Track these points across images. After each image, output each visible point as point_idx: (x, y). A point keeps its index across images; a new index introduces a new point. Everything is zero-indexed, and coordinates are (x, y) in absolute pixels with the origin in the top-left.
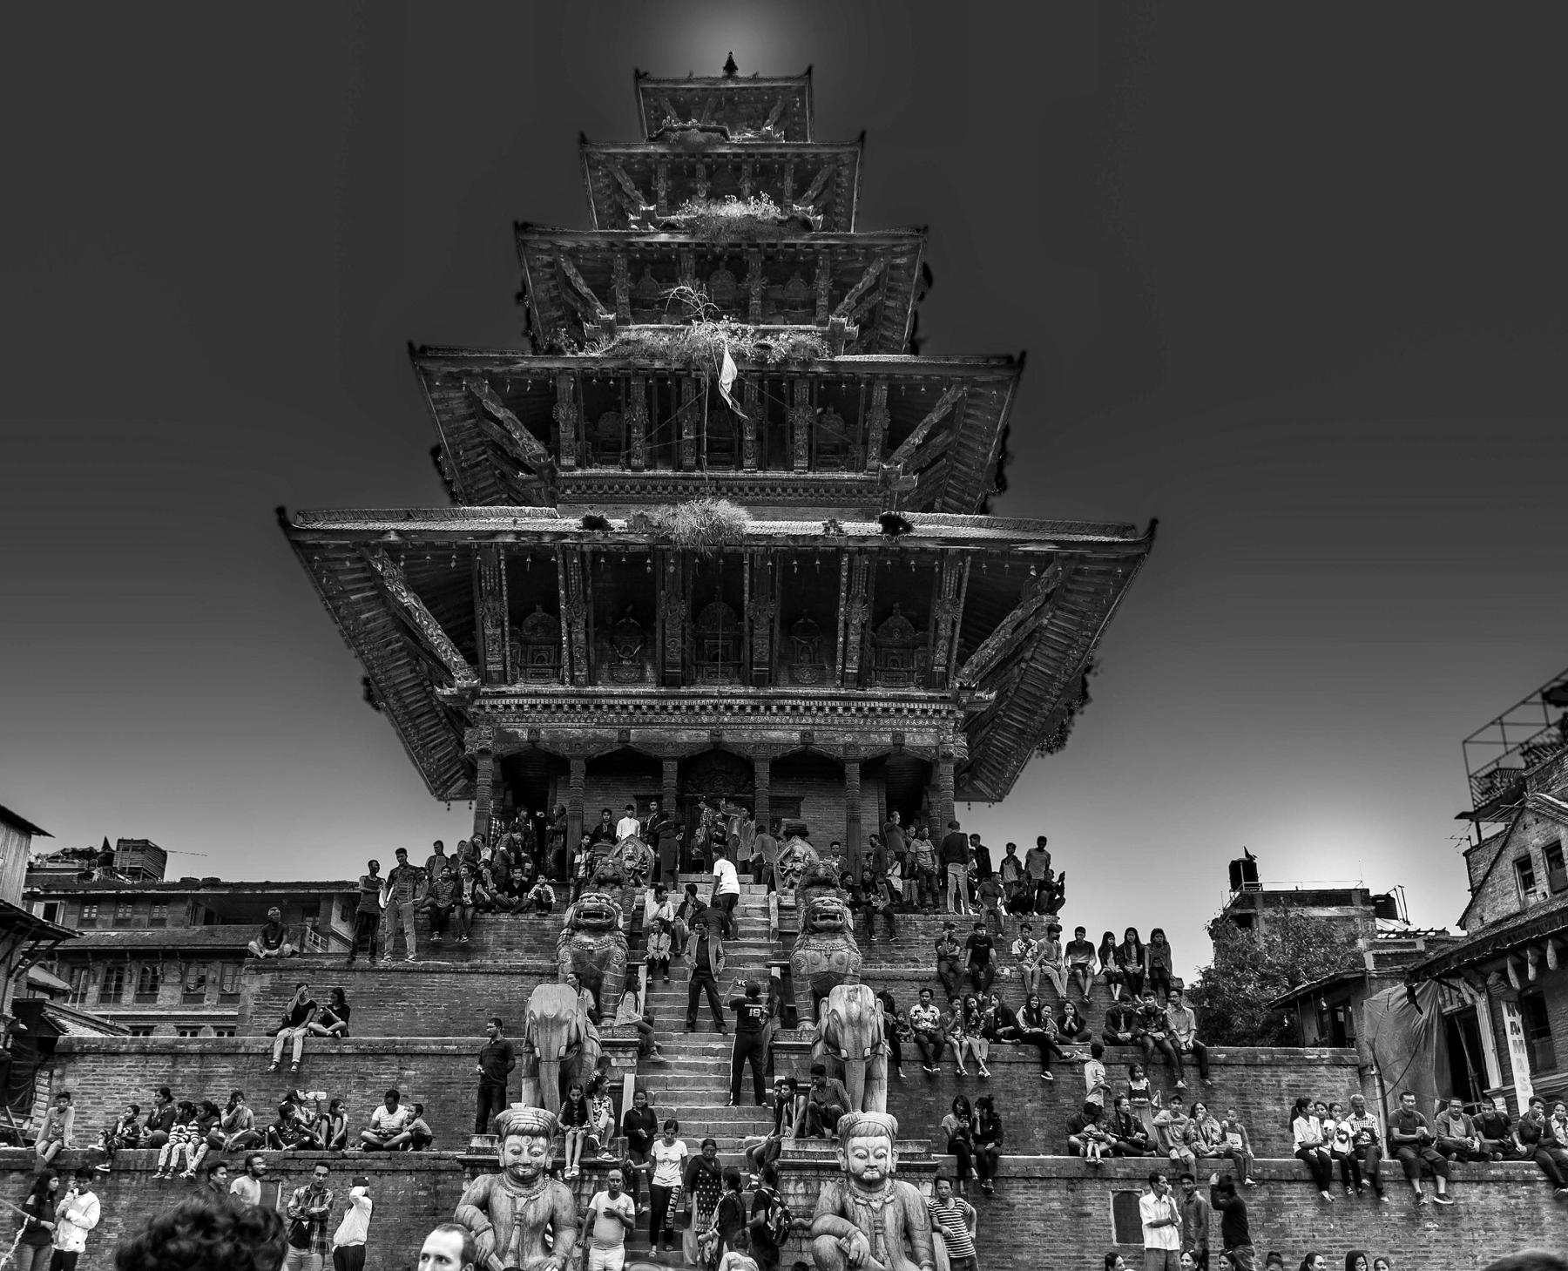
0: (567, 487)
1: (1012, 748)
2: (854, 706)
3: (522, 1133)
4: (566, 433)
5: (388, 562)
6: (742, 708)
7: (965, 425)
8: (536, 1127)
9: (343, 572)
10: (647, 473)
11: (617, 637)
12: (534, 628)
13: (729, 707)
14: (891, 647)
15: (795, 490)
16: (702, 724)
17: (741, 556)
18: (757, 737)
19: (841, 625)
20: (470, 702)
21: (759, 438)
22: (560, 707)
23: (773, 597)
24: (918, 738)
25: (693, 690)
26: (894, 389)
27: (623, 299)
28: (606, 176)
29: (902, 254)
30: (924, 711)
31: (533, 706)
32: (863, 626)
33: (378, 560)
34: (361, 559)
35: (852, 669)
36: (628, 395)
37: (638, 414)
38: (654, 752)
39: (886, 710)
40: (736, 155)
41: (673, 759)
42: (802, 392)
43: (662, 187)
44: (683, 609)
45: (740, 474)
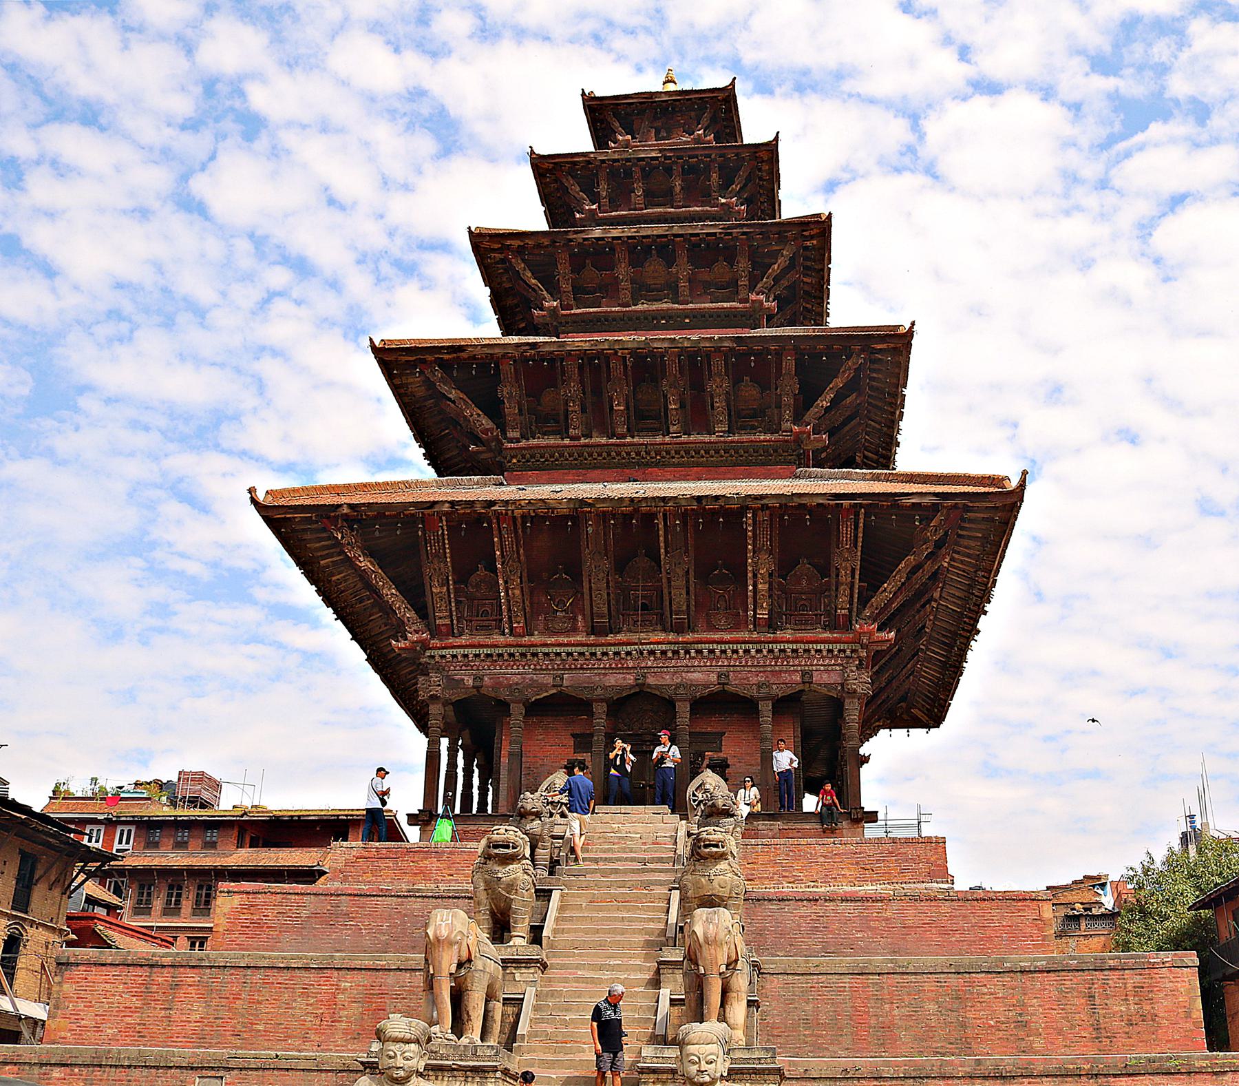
0: (513, 457)
1: (938, 678)
3: (396, 1040)
4: (511, 410)
5: (346, 530)
6: (664, 653)
7: (871, 388)
8: (408, 1036)
9: (310, 541)
10: (583, 441)
12: (478, 586)
13: (652, 652)
15: (717, 452)
16: (628, 668)
17: (653, 516)
19: (750, 575)
21: (682, 406)
23: (687, 551)
24: (825, 676)
25: (619, 637)
27: (566, 287)
28: (556, 181)
29: (812, 237)
30: (830, 651)
32: (771, 575)
33: (338, 530)
34: (324, 530)
35: (763, 614)
37: (574, 388)
38: (585, 695)
39: (793, 651)
41: (602, 701)
42: (718, 364)
43: (603, 189)
44: (606, 564)
45: (667, 439)
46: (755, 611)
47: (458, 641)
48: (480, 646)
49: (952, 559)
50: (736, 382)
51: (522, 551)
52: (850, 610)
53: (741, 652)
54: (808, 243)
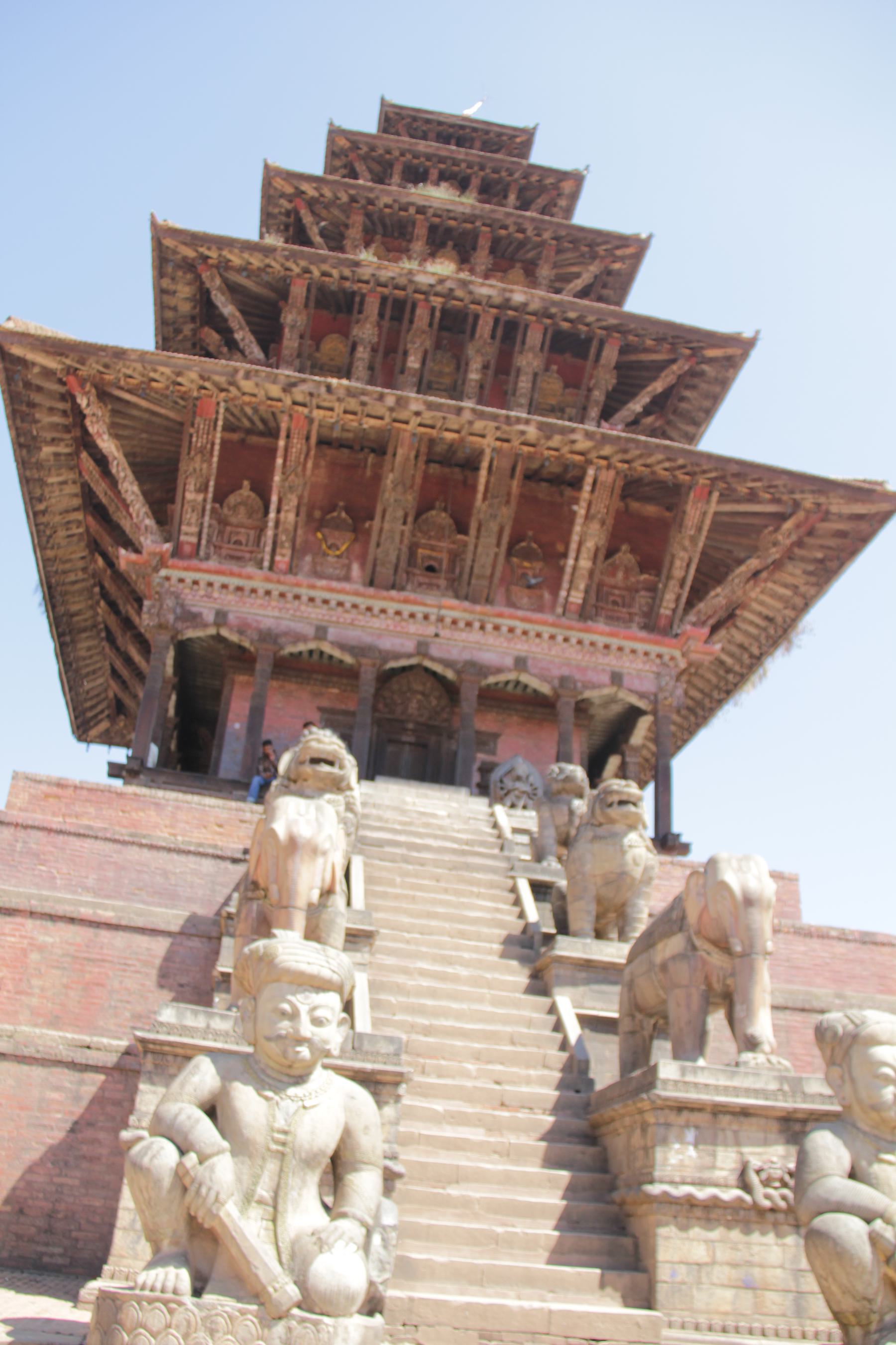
2: (574, 636)
4: (290, 342)
5: (93, 398)
6: (454, 622)
11: (326, 531)
12: (234, 508)
14: (614, 587)
18: (466, 656)
20: (156, 570)
22: (254, 591)
23: (508, 502)
25: (403, 594)
26: (624, 350)
28: (345, 166)
29: (622, 259)
30: (646, 654)
31: (224, 586)
35: (577, 597)
37: (366, 331)
39: (607, 647)
40: (470, 166)
42: (534, 337)
44: (410, 499)
46: (569, 591)
47: (204, 565)
48: (232, 574)
49: (762, 592)
50: (547, 369)
51: (310, 464)
52: (674, 611)
53: (546, 636)
54: (617, 266)
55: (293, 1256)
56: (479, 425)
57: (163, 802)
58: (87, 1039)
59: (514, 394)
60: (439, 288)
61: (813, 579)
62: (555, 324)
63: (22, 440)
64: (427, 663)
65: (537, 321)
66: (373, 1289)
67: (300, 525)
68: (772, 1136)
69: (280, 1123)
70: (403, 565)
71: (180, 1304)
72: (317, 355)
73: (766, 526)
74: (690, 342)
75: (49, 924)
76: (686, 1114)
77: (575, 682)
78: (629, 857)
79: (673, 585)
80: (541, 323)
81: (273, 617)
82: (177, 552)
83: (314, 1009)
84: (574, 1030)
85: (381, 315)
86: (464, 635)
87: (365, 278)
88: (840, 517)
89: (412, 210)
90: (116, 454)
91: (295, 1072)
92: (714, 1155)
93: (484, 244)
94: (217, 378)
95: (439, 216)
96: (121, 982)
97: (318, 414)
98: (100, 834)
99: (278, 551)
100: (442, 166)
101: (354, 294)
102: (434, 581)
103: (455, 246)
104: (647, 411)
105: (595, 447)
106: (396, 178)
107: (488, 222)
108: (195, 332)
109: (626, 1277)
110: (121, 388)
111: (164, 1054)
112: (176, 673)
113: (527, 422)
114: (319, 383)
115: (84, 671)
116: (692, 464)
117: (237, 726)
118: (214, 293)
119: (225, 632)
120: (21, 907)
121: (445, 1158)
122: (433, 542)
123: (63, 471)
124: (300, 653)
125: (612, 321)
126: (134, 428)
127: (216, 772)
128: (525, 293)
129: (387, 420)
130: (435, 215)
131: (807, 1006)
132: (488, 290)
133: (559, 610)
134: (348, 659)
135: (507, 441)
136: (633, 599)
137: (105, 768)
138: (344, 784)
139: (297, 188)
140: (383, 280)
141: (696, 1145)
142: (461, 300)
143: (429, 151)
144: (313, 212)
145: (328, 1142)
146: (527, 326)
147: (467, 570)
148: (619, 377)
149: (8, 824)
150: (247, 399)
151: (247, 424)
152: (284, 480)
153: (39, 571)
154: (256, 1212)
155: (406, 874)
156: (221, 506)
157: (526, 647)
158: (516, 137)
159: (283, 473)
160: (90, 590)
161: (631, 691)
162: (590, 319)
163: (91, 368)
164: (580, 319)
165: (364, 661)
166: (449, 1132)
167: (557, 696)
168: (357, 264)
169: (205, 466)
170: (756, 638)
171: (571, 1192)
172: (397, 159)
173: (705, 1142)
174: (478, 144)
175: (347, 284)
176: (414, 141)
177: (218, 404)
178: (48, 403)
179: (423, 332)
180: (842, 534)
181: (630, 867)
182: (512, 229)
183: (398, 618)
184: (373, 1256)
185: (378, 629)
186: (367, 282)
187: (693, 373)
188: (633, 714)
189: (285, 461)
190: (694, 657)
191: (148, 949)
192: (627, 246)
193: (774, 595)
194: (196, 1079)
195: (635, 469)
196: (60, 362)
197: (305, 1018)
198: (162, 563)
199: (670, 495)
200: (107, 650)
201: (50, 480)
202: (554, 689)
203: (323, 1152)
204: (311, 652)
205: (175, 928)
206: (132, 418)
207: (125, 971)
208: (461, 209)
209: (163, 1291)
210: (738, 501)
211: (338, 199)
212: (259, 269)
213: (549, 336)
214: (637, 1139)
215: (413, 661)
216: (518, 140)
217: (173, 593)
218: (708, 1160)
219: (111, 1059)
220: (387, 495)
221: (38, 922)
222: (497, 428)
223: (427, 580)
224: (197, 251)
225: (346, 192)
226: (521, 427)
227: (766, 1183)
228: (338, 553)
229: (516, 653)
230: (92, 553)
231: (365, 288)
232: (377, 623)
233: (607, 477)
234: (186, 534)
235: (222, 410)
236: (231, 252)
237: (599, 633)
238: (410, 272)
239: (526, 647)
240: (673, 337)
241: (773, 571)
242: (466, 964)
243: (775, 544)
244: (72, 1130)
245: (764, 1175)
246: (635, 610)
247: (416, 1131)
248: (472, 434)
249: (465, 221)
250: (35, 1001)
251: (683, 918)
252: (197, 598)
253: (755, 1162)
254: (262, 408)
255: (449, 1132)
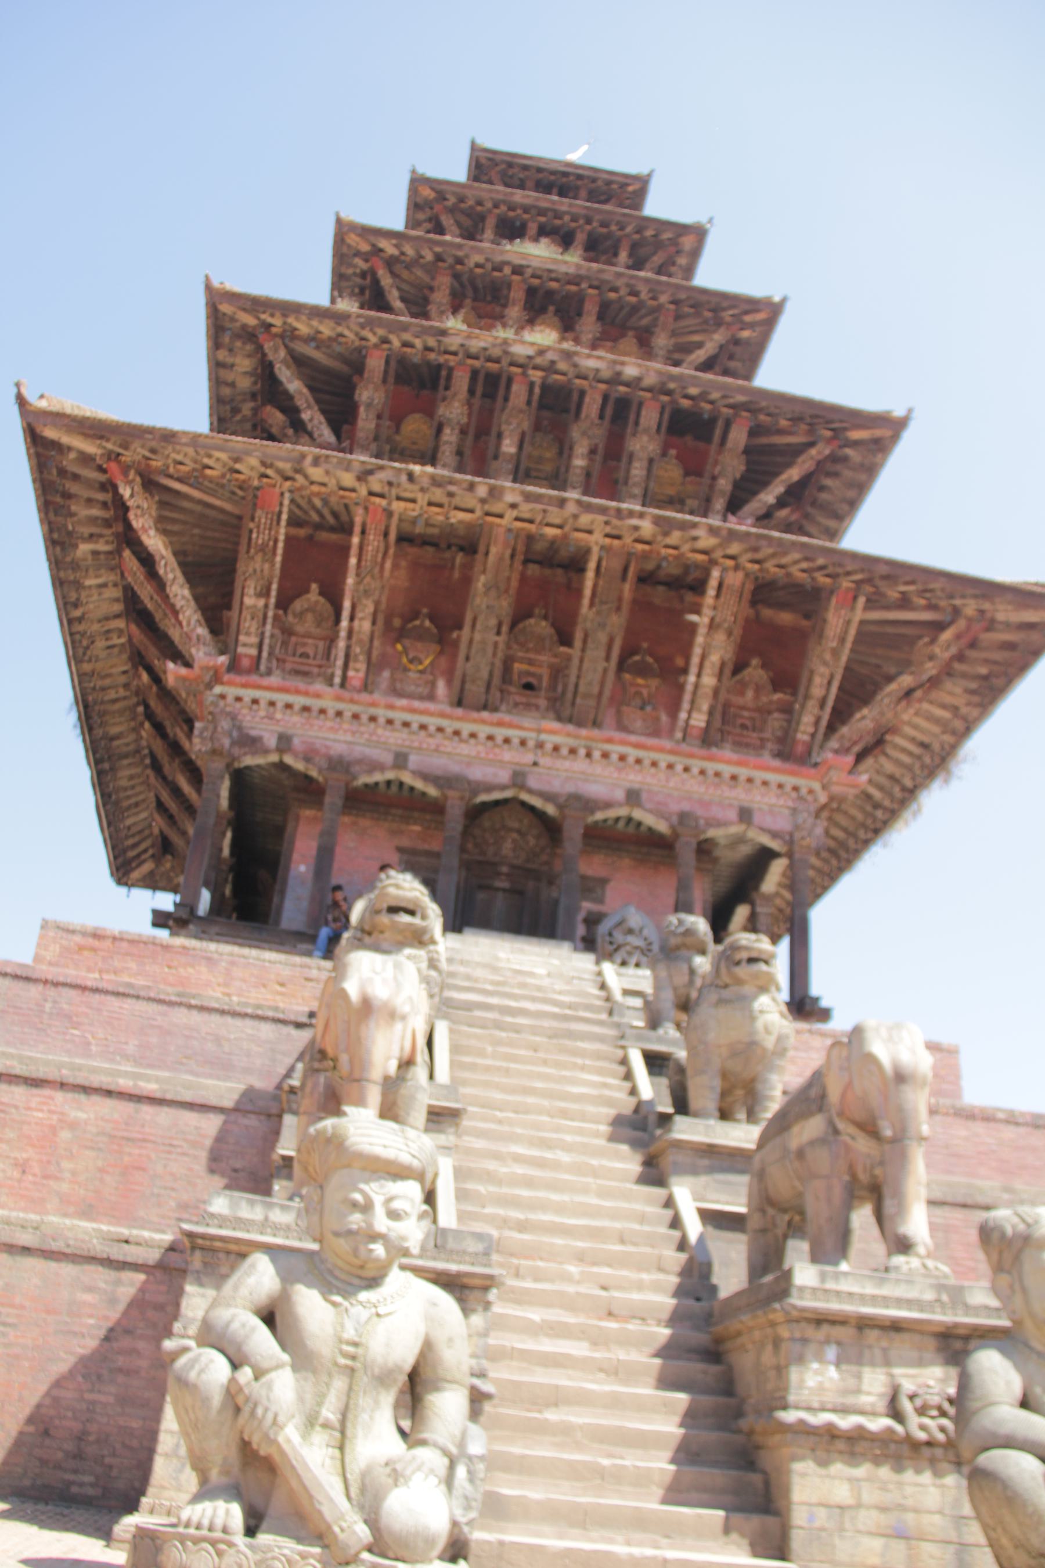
2: (696, 765)
4: (366, 422)
5: (138, 488)
6: (556, 749)
11: (407, 642)
12: (301, 615)
14: (743, 708)
16: (501, 761)
18: (570, 788)
20: (209, 686)
22: (322, 711)
23: (618, 609)
25: (496, 716)
28: (430, 220)
29: (752, 326)
30: (780, 786)
31: (288, 706)
35: (699, 720)
36: (447, 388)
37: (454, 410)
39: (734, 778)
40: (574, 219)
42: (650, 417)
44: (505, 605)
46: (690, 713)
47: (266, 681)
48: (297, 692)
49: (916, 714)
50: (664, 454)
51: (388, 565)
52: (813, 736)
53: (663, 765)
54: (745, 334)
55: (363, 1490)
56: (585, 519)
57: (216, 956)
58: (125, 1232)
59: (626, 483)
60: (539, 361)
61: (976, 699)
62: (673, 402)
63: (56, 536)
64: (525, 797)
65: (653, 398)
66: (456, 1531)
67: (377, 634)
68: (928, 1355)
69: (350, 1333)
70: (496, 681)
71: (231, 1544)
72: (398, 438)
73: (920, 637)
74: (831, 422)
75: (82, 1097)
76: (826, 1328)
77: (697, 819)
78: (759, 1024)
79: (812, 706)
80: (658, 400)
81: (345, 742)
82: (234, 666)
83: (390, 1200)
84: (694, 1228)
85: (471, 392)
86: (567, 764)
87: (453, 348)
88: (1008, 626)
89: (507, 270)
90: (164, 552)
91: (369, 1273)
92: (859, 1377)
93: (591, 309)
94: (280, 465)
95: (539, 277)
96: (165, 1166)
97: (397, 506)
98: (142, 993)
99: (351, 665)
100: (543, 219)
101: (439, 367)
102: (533, 701)
103: (557, 312)
104: (781, 502)
105: (720, 545)
106: (489, 234)
107: (596, 283)
108: (255, 411)
109: (755, 1521)
110: (171, 477)
111: (214, 1250)
112: (231, 806)
113: (641, 515)
114: (400, 470)
115: (125, 804)
116: (834, 564)
117: (302, 868)
118: (277, 366)
119: (288, 760)
120: (50, 1077)
121: (542, 1377)
122: (531, 656)
123: (103, 571)
124: (377, 784)
125: (741, 398)
126: (185, 523)
127: (277, 922)
128: (639, 366)
129: (479, 513)
130: (533, 276)
131: (969, 1201)
132: (595, 361)
133: (679, 735)
134: (432, 791)
135: (618, 537)
136: (765, 722)
137: (149, 917)
138: (426, 938)
139: (373, 245)
140: (473, 351)
141: (838, 1364)
142: (564, 374)
143: (527, 202)
144: (393, 274)
145: (406, 1356)
146: (640, 405)
147: (571, 688)
148: (748, 463)
149: (36, 981)
150: (315, 488)
151: (315, 517)
152: (358, 583)
153: (74, 687)
154: (320, 1437)
155: (498, 1042)
156: (285, 612)
157: (639, 778)
158: (627, 185)
159: (358, 575)
160: (132, 709)
161: (763, 829)
162: (715, 395)
163: (136, 453)
164: (703, 396)
165: (451, 793)
166: (547, 1345)
167: (676, 835)
168: (444, 333)
169: (267, 566)
170: (909, 768)
171: (690, 1418)
172: (490, 211)
173: (849, 1361)
174: (583, 193)
175: (432, 356)
176: (509, 190)
177: (282, 494)
178: (85, 493)
179: (521, 411)
180: (1010, 646)
181: (761, 1036)
182: (623, 292)
183: (490, 744)
184: (457, 1491)
185: (468, 756)
186: (455, 354)
187: (834, 459)
188: (764, 857)
189: (359, 560)
190: (836, 789)
191: (197, 1128)
192: (757, 311)
193: (930, 718)
194: (251, 1281)
195: (768, 571)
196: (100, 446)
197: (379, 1211)
198: (217, 678)
199: (808, 600)
200: (153, 780)
201: (88, 582)
202: (672, 827)
203: (398, 1368)
204: (389, 783)
205: (228, 1103)
206: (183, 510)
207: (170, 1152)
208: (563, 269)
209: (211, 1529)
210: (887, 608)
211: (422, 257)
212: (330, 339)
213: (666, 416)
214: (768, 1357)
215: (508, 794)
216: (630, 189)
217: (229, 714)
218: (851, 1382)
219: (153, 1256)
220: (478, 601)
221: (70, 1095)
222: (607, 523)
223: (524, 700)
224: (258, 318)
225: (431, 249)
226: (634, 522)
227: (921, 1411)
228: (421, 667)
229: (628, 785)
230: (135, 667)
231: (452, 360)
232: (466, 749)
233: (735, 579)
234: (245, 645)
235: (286, 502)
236: (297, 319)
237: (726, 761)
238: (505, 342)
239: (639, 778)
240: (812, 417)
241: (929, 688)
242: (568, 1148)
243: (931, 657)
244: (107, 1339)
245: (918, 1402)
246: (767, 735)
247: (508, 1344)
248: (577, 530)
249: (569, 283)
250: (65, 1187)
251: (823, 1096)
252: (257, 719)
253: (908, 1386)
254: (333, 500)
255: (547, 1345)
